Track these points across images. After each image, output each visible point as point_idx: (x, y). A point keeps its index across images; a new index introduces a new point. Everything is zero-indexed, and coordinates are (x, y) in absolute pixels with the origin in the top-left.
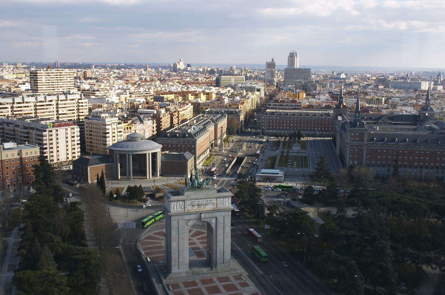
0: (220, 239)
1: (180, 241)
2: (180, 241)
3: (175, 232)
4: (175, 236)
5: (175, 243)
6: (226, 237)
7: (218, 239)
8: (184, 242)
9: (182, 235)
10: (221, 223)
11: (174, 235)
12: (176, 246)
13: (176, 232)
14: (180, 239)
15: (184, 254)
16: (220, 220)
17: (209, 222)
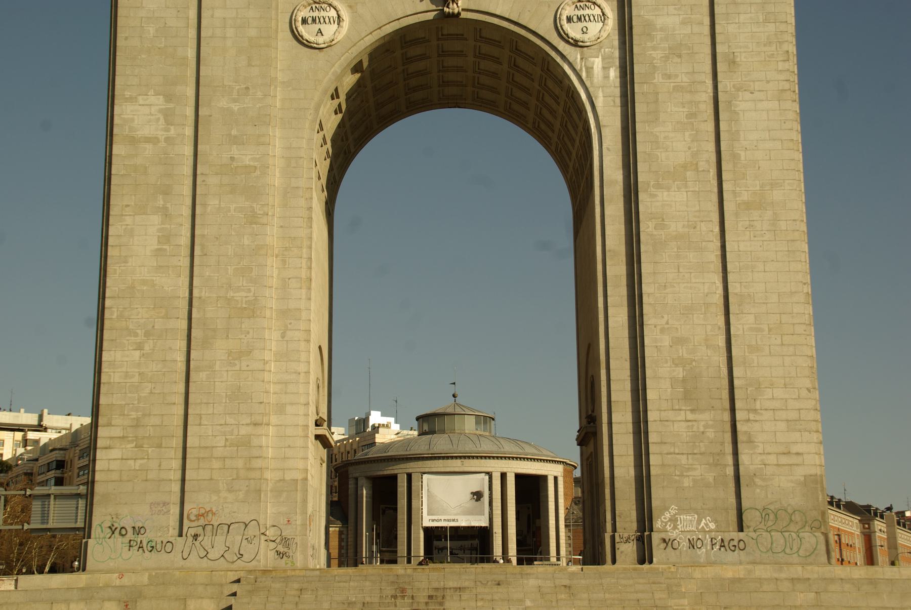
0: (675, 227)
1: (210, 204)
2: (213, 202)
3: (159, 101)
4: (153, 140)
5: (156, 219)
6: (748, 206)
7: (647, 227)
8: (253, 219)
9: (235, 141)
10: (676, 51)
11: (146, 132)
12: (159, 252)
13: (169, 98)
14: (209, 180)
15: (247, 353)
16: (660, 22)
17: (545, 28)
